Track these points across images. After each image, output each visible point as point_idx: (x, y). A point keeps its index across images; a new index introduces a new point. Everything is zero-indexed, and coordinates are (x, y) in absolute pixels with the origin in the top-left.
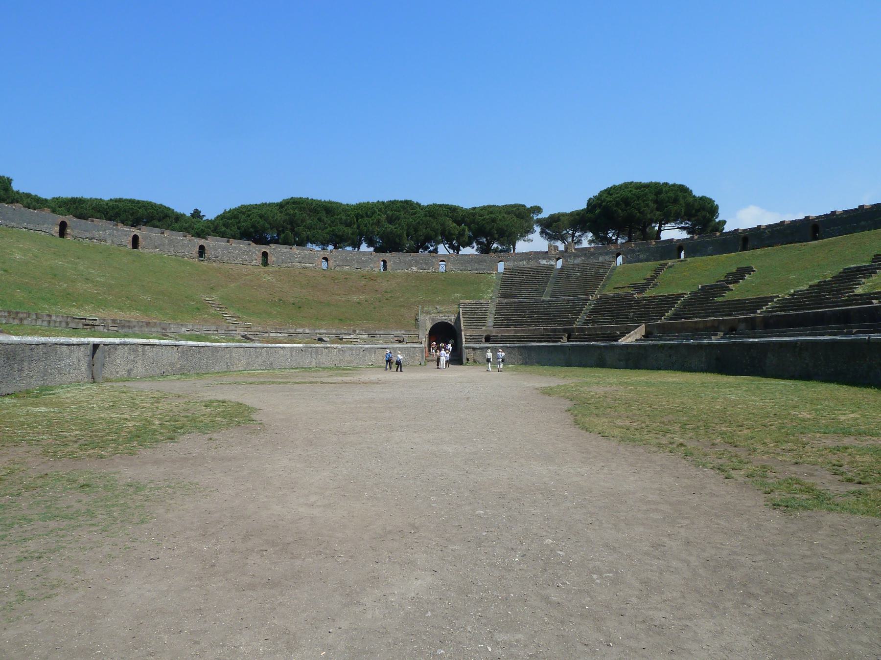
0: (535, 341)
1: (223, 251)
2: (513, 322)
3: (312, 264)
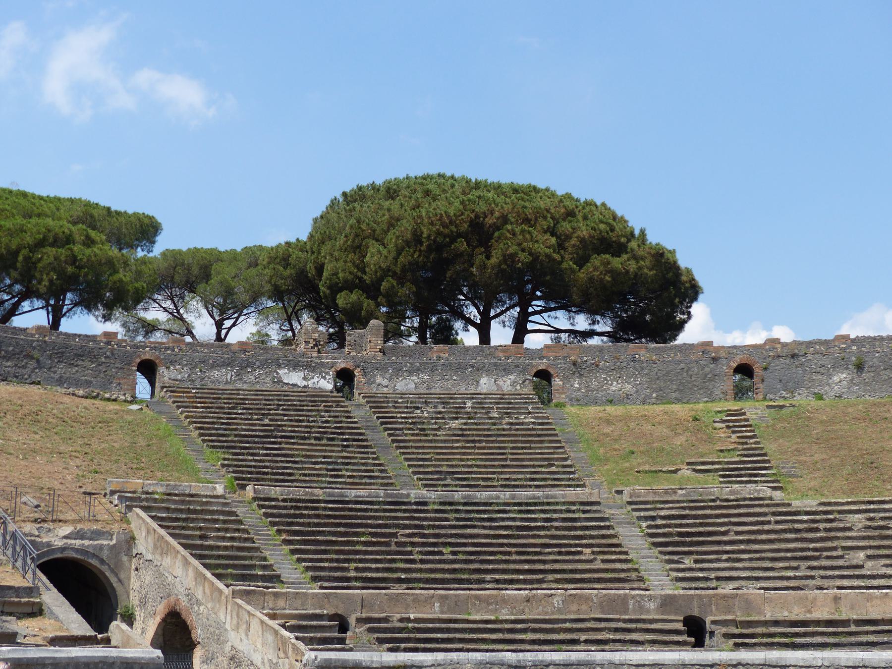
0: (605, 642)
2: (377, 570)
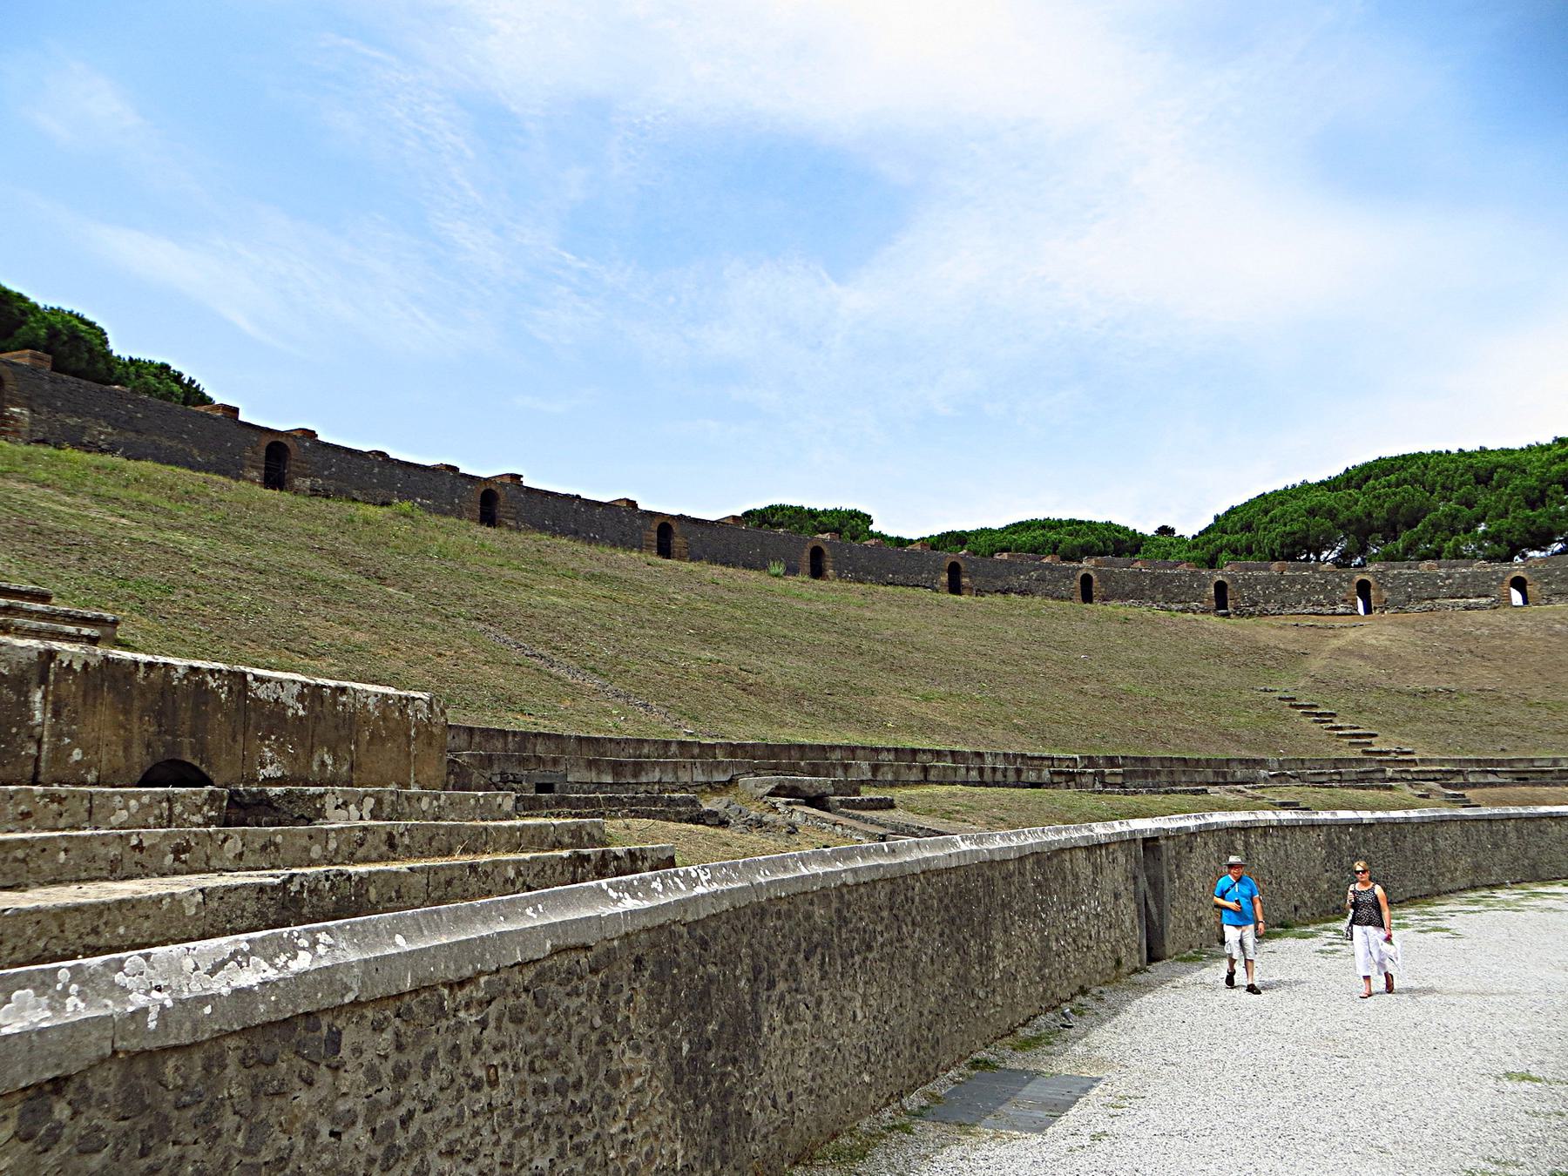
1: (1267, 589)
3: (1486, 596)
